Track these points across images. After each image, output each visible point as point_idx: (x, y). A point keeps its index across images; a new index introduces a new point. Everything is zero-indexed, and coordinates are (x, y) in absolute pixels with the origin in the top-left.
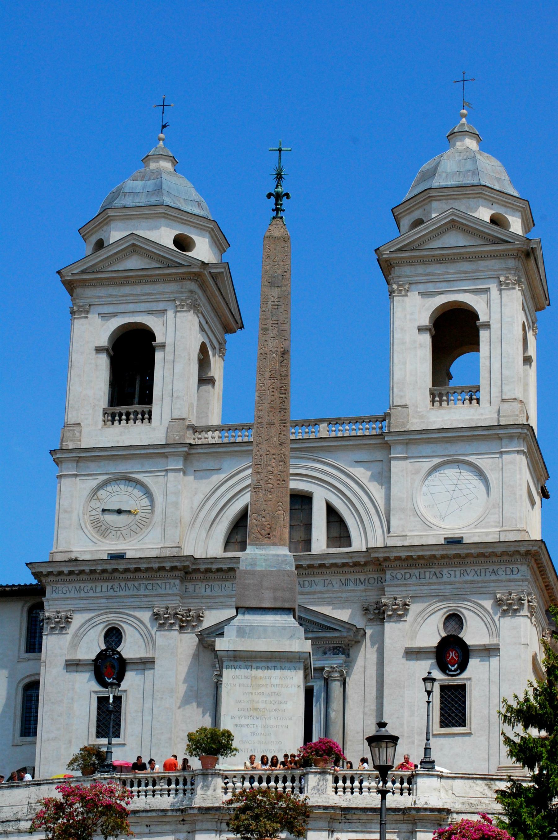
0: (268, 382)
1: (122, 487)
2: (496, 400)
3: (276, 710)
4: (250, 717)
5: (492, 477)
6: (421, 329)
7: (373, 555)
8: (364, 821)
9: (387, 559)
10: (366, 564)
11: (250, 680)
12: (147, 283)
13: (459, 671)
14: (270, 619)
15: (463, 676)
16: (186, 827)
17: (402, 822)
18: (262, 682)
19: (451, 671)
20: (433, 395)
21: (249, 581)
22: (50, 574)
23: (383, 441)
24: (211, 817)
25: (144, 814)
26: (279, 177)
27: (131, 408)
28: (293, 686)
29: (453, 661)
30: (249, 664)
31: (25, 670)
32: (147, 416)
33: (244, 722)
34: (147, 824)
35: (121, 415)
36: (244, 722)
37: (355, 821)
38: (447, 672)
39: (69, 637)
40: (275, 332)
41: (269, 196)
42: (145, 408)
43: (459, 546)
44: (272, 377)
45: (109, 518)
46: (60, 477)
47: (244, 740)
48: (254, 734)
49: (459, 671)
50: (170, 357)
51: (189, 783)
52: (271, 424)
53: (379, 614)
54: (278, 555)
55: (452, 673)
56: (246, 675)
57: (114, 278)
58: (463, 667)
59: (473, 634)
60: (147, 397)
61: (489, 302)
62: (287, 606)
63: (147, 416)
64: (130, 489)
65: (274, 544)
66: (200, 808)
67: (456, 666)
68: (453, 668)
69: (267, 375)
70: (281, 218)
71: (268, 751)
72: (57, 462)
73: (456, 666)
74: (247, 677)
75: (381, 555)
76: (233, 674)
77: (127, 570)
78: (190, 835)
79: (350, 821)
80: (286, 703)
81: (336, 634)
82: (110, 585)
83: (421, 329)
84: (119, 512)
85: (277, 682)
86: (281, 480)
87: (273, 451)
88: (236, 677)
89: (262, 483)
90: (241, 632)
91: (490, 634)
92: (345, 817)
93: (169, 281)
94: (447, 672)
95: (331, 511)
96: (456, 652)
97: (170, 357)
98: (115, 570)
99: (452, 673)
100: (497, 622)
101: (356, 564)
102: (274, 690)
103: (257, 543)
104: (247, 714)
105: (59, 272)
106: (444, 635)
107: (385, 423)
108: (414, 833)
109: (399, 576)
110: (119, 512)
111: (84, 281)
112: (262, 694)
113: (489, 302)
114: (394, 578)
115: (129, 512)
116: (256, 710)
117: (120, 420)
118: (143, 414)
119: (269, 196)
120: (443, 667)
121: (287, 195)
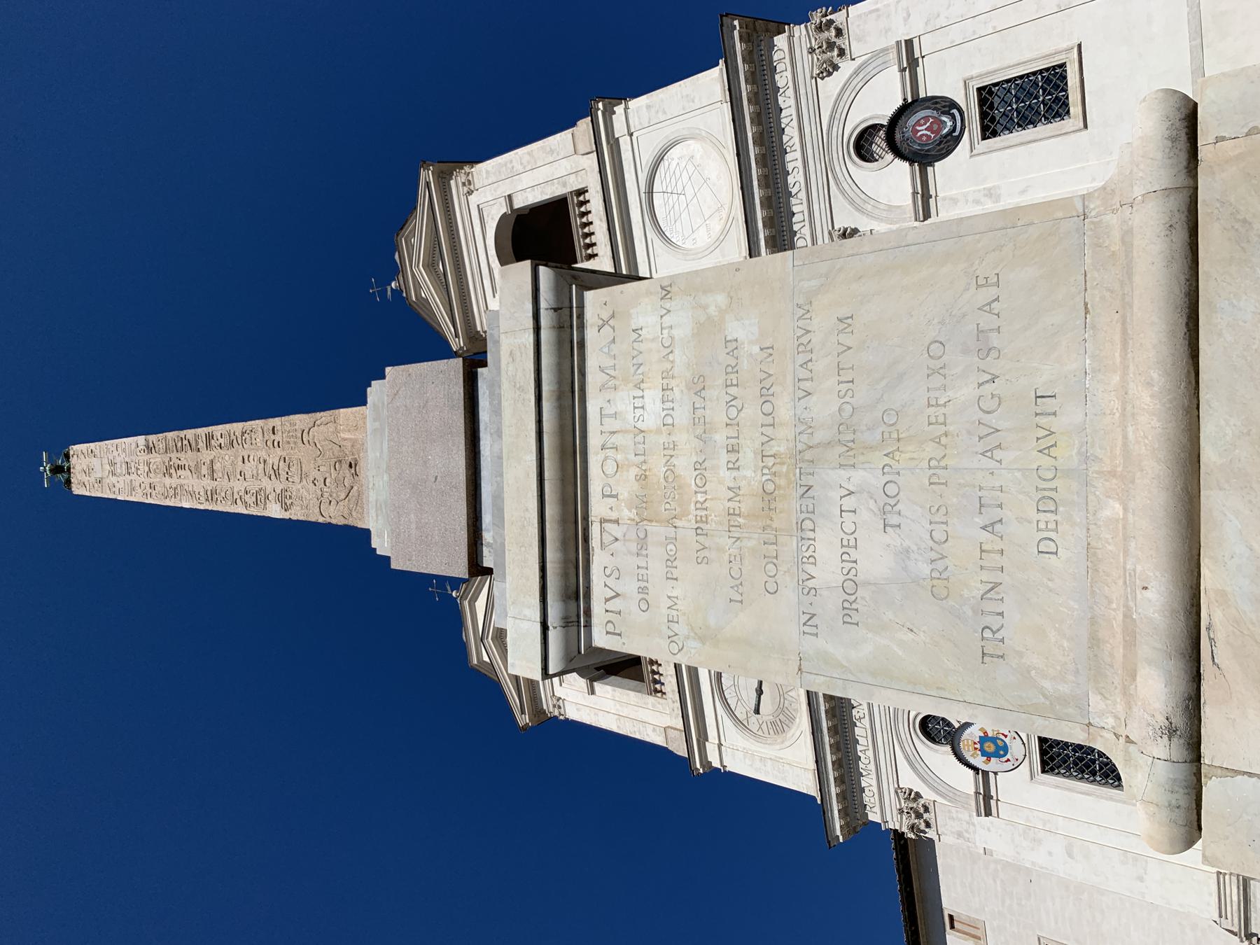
3: (766, 396)
4: (803, 529)
11: (653, 528)
13: (955, 111)
15: (961, 101)
18: (658, 468)
19: (954, 130)
21: (413, 526)
28: (667, 320)
29: (935, 127)
30: (595, 531)
33: (828, 570)
36: (828, 570)
38: (956, 134)
39: (939, 799)
47: (925, 569)
49: (955, 111)
55: (959, 124)
56: (633, 547)
58: (946, 106)
67: (944, 118)
68: (949, 124)
71: (991, 420)
73: (944, 118)
74: (643, 542)
76: (635, 608)
80: (733, 346)
85: (652, 397)
86: (273, 437)
88: (643, 590)
91: (885, 66)
94: (956, 134)
96: (918, 123)
99: (959, 124)
100: (859, 61)
102: (682, 415)
104: (790, 545)
106: (890, 156)
112: (699, 466)
116: (768, 497)
117: (658, 673)
120: (948, 144)
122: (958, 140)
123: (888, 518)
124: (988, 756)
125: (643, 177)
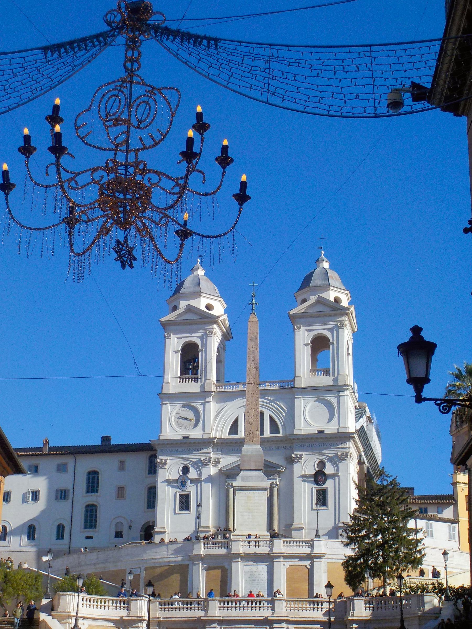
2: (336, 375)
7: (289, 437)
9: (294, 439)
10: (286, 440)
22: (159, 444)
31: (149, 481)
32: (196, 380)
35: (186, 379)
40: (253, 359)
43: (323, 434)
45: (182, 421)
48: (248, 518)
53: (291, 461)
54: (256, 449)
58: (324, 483)
59: (329, 469)
65: (255, 444)
70: (254, 313)
75: (291, 438)
77: (190, 443)
81: (274, 469)
82: (183, 448)
84: (186, 419)
87: (253, 407)
90: (243, 479)
95: (271, 418)
98: (185, 443)
101: (281, 441)
103: (249, 444)
107: (292, 383)
109: (299, 446)
110: (186, 419)
111: (170, 323)
114: (297, 446)
118: (195, 378)
120: (317, 482)
121: (256, 304)
122: (317, 485)
123: (248, 518)
124: (182, 482)
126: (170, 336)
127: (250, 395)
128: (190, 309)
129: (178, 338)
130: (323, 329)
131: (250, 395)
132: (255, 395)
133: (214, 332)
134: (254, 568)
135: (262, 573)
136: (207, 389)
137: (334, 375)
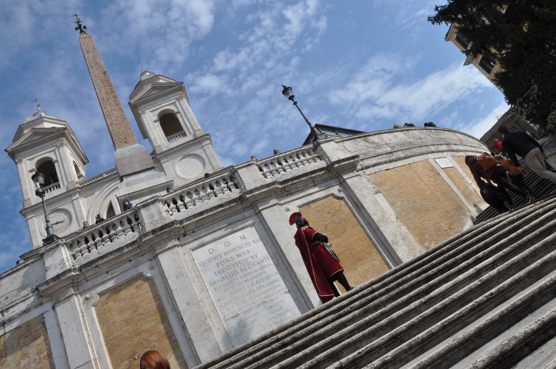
0: (101, 85)
1: (56, 214)
5: (203, 155)
6: (155, 121)
8: (301, 188)
12: (44, 143)
14: (142, 175)
16: (147, 257)
17: (329, 179)
20: (169, 140)
23: (156, 159)
24: (167, 236)
25: (101, 262)
26: (78, 22)
27: (50, 186)
32: (58, 186)
34: (106, 270)
37: (294, 191)
41: (77, 29)
42: (56, 184)
44: (102, 82)
46: (27, 220)
50: (60, 164)
51: (133, 220)
52: (108, 99)
57: (29, 146)
60: (57, 180)
61: (176, 106)
62: (149, 167)
63: (58, 186)
64: (59, 214)
65: (130, 144)
66: (154, 232)
69: (99, 82)
72: (24, 215)
78: (154, 261)
79: (290, 192)
83: (155, 121)
84: (57, 223)
87: (114, 108)
89: (114, 122)
90: (128, 185)
92: (285, 190)
93: (53, 140)
97: (60, 164)
105: (6, 150)
108: (343, 183)
113: (176, 106)
115: (61, 222)
118: (56, 186)
119: (77, 29)
121: (85, 27)
125: (193, 152)
126: (21, 160)
127: (105, 98)
128: (36, 133)
129: (29, 160)
130: (166, 105)
131: (105, 98)
132: (111, 96)
133: (64, 143)
134: (219, 246)
135: (245, 250)
136: (70, 189)
137: (190, 134)
